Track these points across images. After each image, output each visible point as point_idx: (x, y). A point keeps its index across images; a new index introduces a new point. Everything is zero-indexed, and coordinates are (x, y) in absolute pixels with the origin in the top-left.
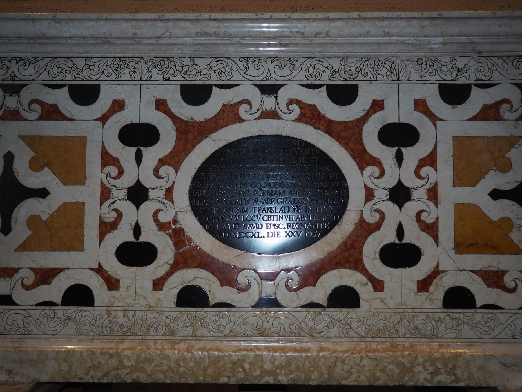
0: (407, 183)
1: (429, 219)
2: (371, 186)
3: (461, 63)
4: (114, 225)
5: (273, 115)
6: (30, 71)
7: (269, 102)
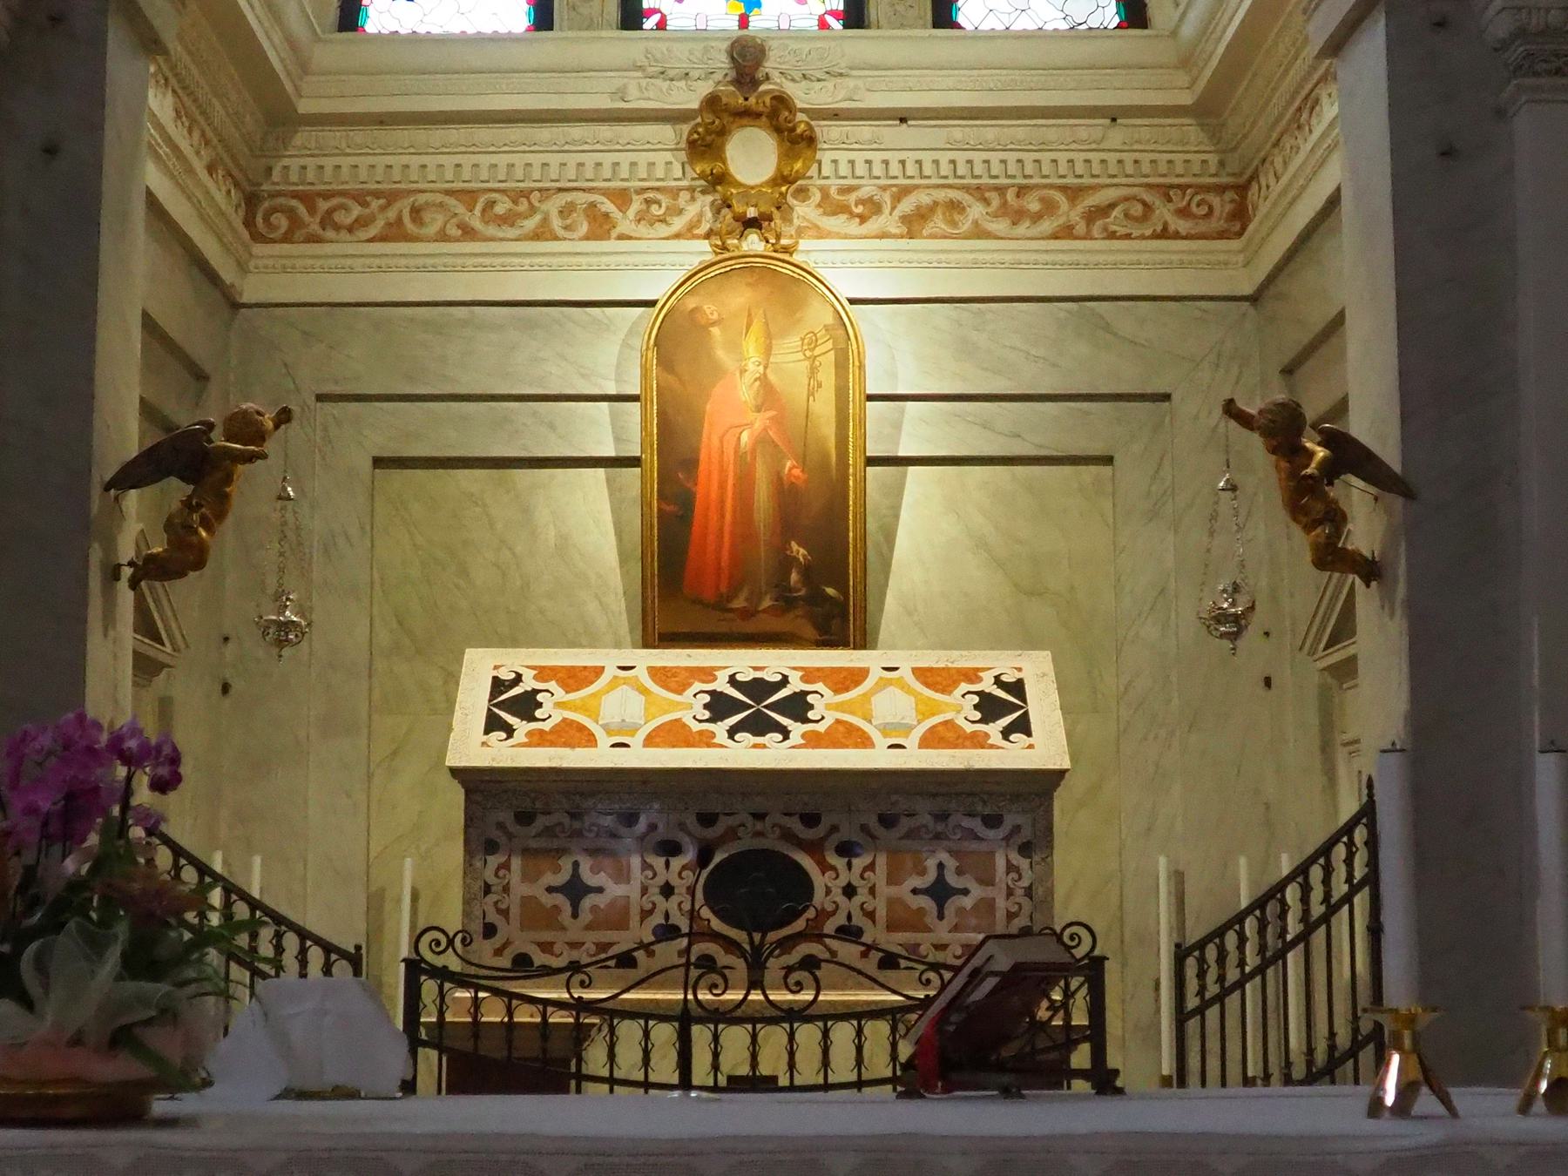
0: (854, 883)
2: (829, 885)
4: (651, 912)
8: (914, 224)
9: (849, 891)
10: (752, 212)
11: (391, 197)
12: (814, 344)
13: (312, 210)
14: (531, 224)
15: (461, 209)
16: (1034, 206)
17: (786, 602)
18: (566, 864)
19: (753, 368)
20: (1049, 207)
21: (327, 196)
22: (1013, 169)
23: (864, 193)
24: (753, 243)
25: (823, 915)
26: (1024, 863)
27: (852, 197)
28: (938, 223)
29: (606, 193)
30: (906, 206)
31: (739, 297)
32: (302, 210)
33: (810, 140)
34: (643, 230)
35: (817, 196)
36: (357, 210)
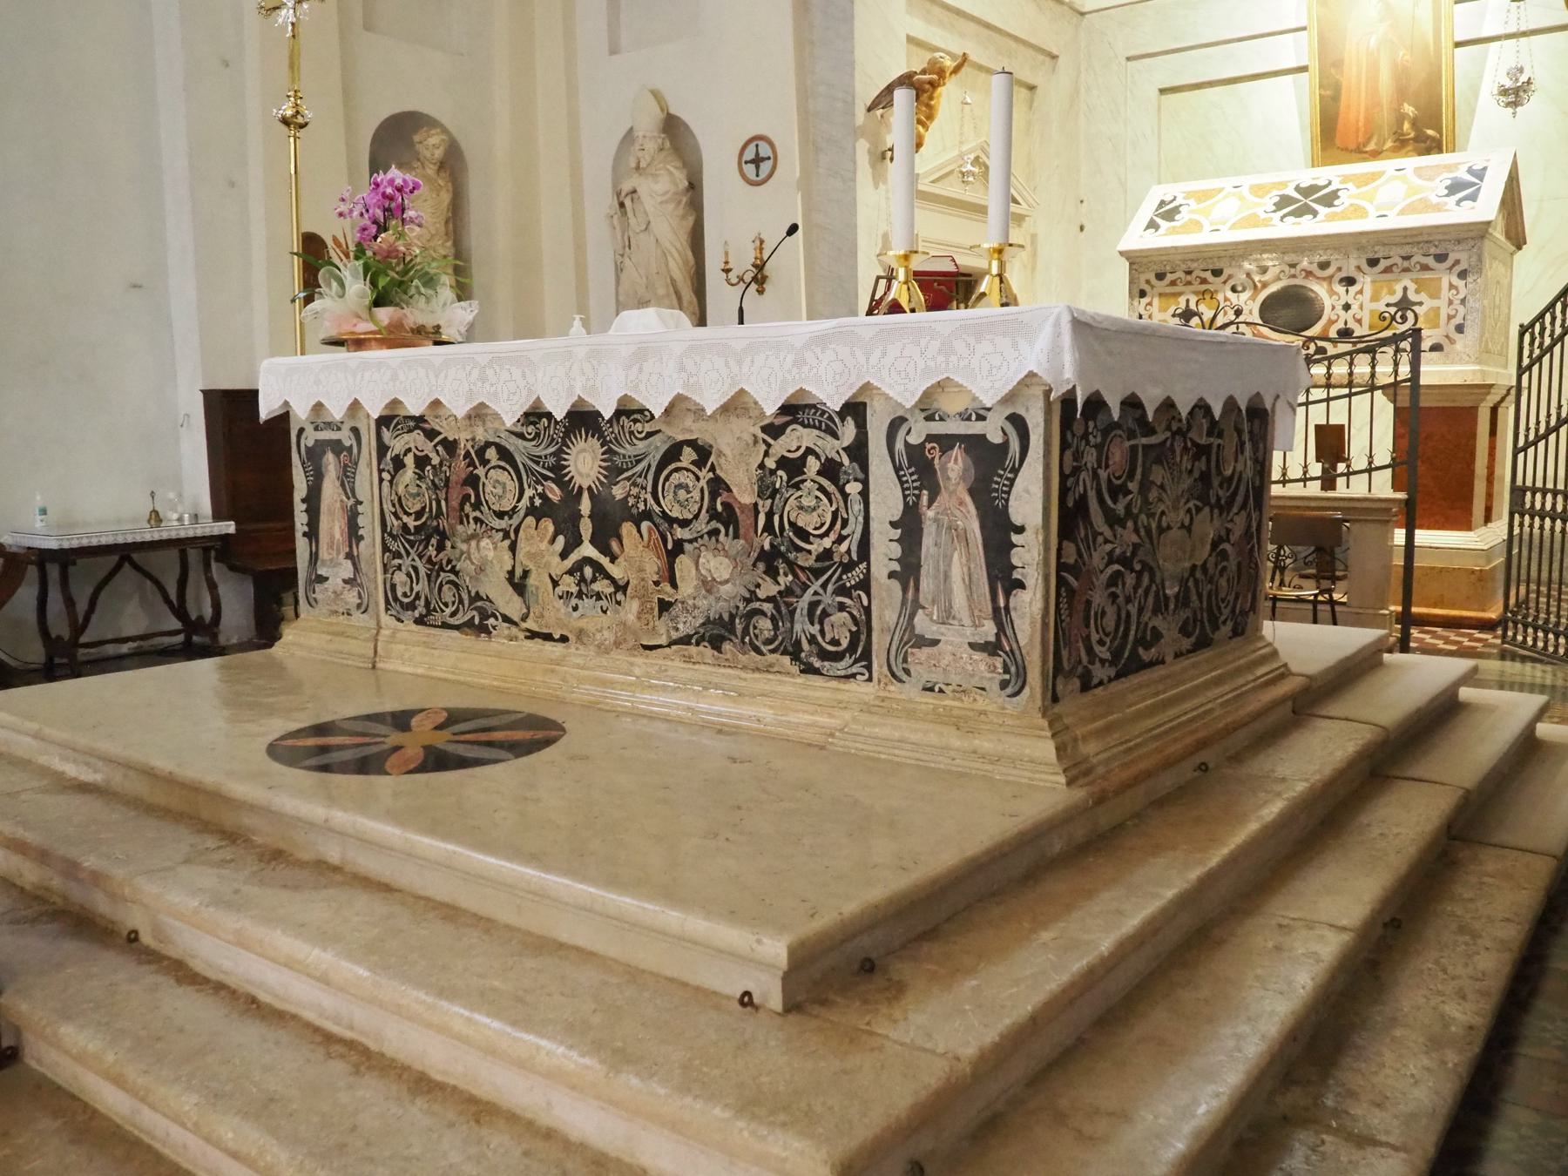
1: (1358, 317)
3: (1377, 248)
5: (1294, 276)
6: (1196, 265)
7: (1293, 271)
9: (1347, 307)
18: (1182, 300)
25: (1331, 322)
26: (1460, 283)
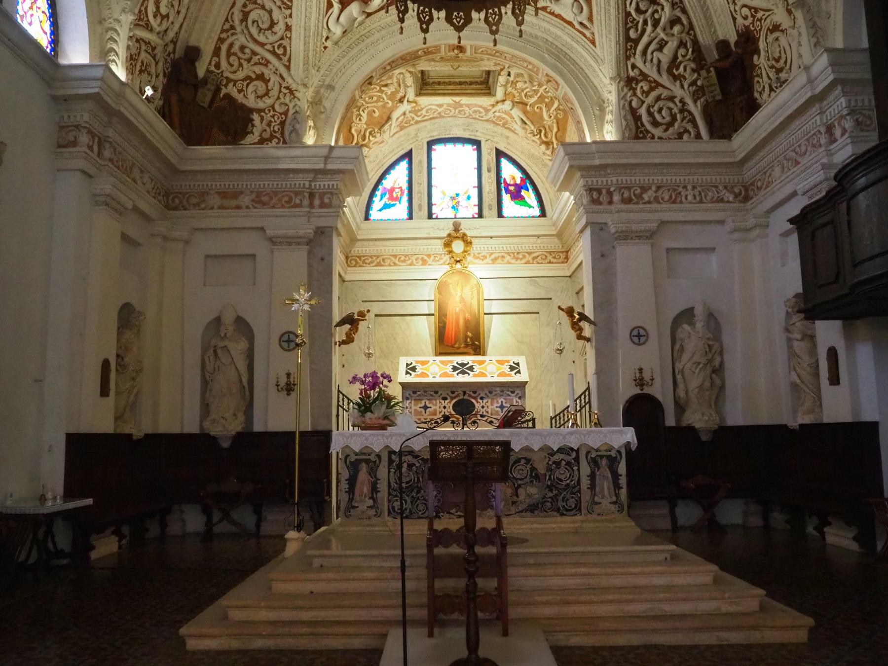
8: (494, 260)
10: (458, 259)
11: (378, 257)
12: (472, 288)
13: (360, 259)
14: (409, 262)
15: (393, 259)
16: (521, 256)
17: (467, 345)
19: (459, 294)
20: (524, 257)
21: (364, 256)
22: (516, 248)
23: (483, 254)
24: (458, 266)
27: (480, 255)
28: (499, 261)
29: (425, 255)
30: (493, 257)
31: (456, 278)
32: (358, 259)
33: (471, 243)
34: (434, 263)
35: (472, 255)
36: (370, 260)
